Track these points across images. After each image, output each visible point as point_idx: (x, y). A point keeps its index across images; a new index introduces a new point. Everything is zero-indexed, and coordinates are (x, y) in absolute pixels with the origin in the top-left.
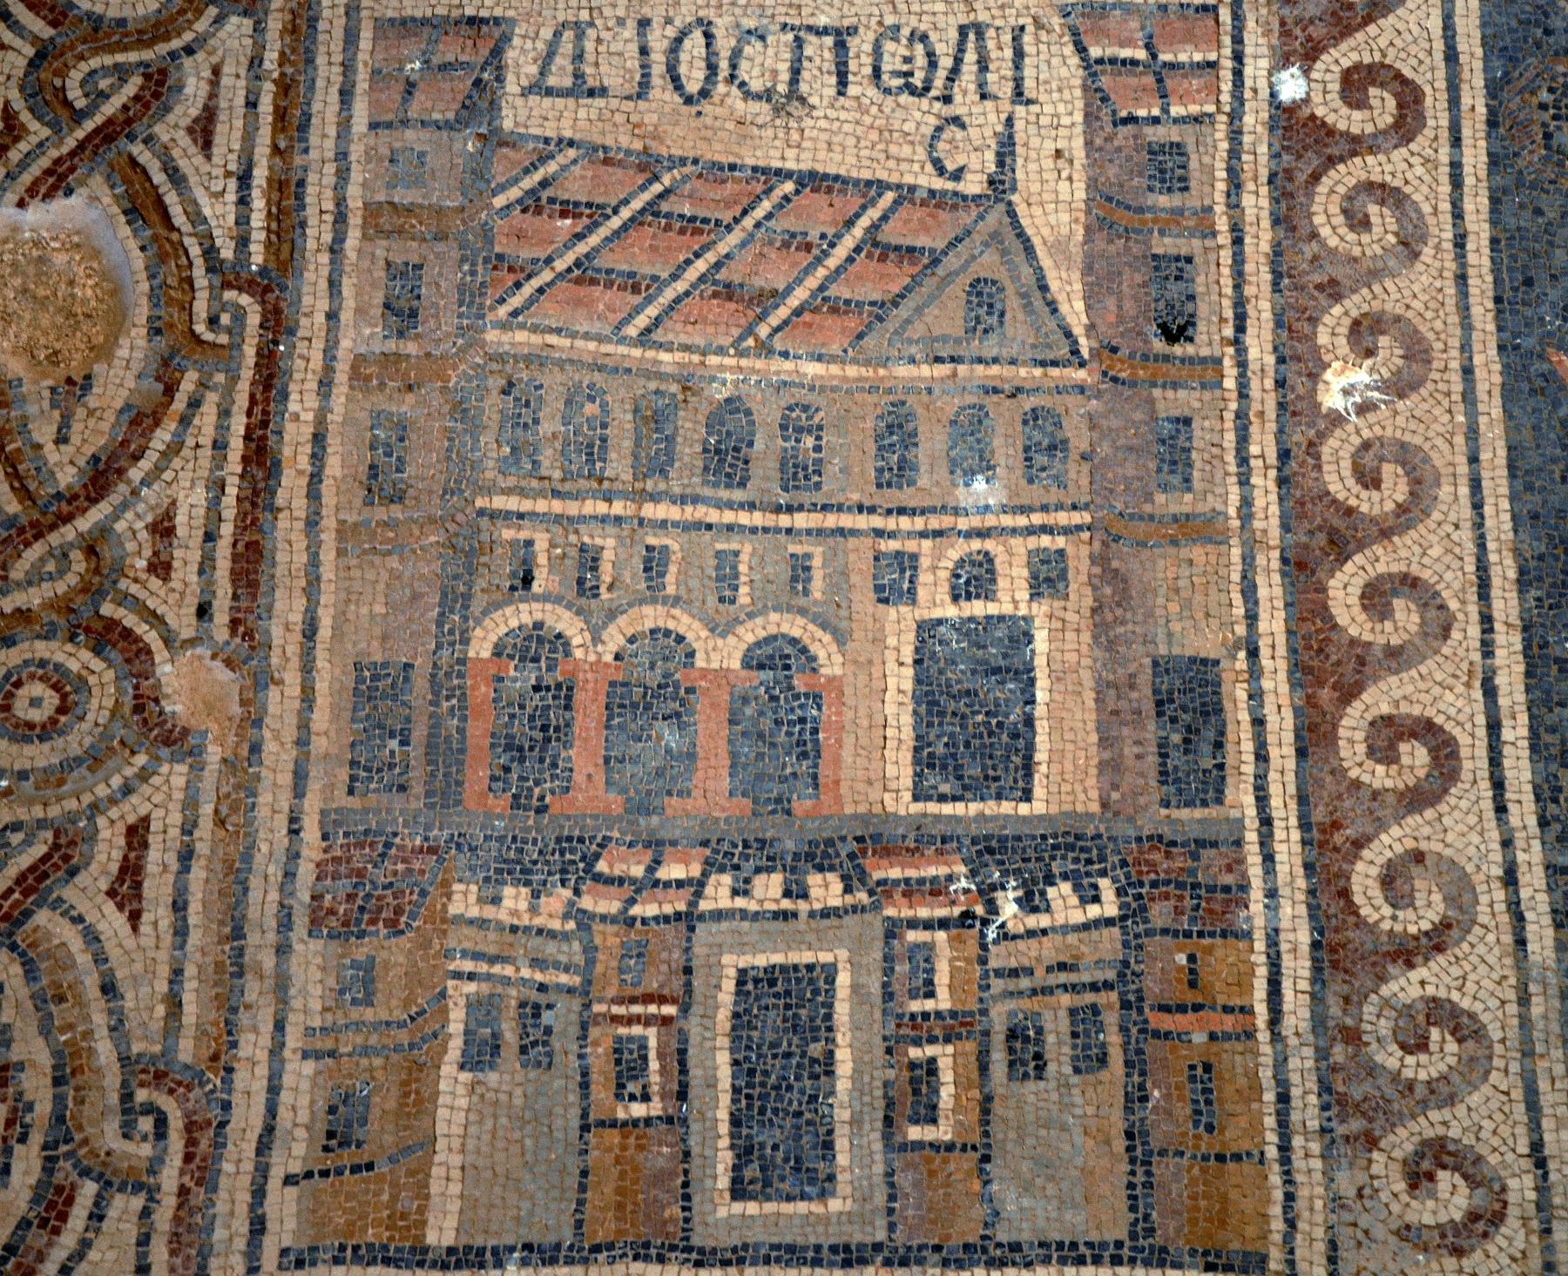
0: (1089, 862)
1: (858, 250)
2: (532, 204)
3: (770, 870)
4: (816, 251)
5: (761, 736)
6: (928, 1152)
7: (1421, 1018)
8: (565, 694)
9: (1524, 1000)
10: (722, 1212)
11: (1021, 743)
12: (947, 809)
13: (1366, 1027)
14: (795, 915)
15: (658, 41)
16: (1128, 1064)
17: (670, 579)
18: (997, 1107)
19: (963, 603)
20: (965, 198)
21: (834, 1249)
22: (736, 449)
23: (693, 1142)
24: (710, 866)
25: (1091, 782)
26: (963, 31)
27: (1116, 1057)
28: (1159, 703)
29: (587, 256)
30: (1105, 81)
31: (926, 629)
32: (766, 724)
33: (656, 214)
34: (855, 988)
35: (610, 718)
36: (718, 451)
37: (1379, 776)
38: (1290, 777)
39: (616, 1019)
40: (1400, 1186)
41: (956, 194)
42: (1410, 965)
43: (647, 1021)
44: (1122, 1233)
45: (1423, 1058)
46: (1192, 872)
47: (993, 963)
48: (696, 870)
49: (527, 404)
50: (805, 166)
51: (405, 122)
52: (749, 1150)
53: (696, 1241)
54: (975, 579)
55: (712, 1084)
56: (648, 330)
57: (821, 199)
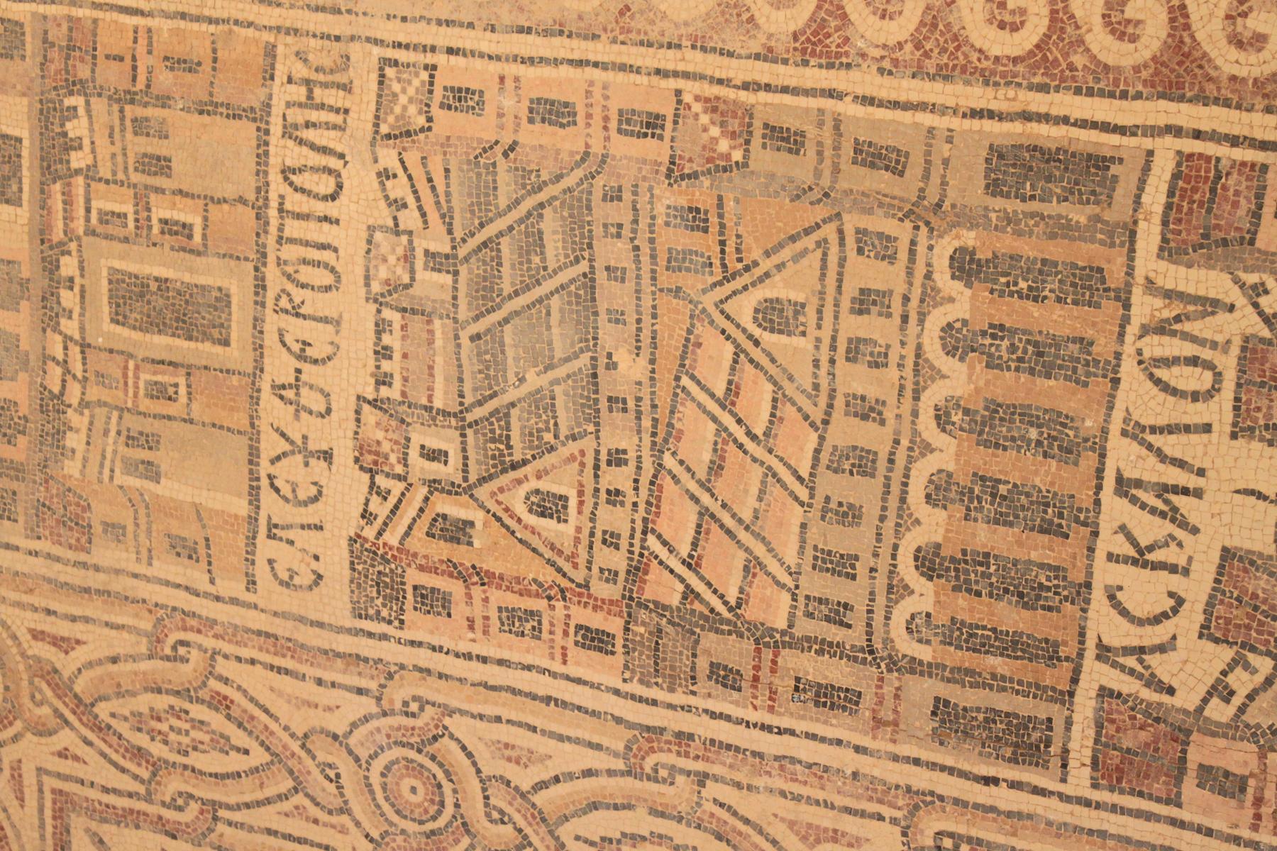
10: (236, 354)
12: (26, 188)
21: (257, 294)
24: (56, 329)
25: (11, 100)
34: (122, 258)
39: (136, 395)
43: (137, 377)
44: (254, 126)
47: (109, 177)
48: (59, 338)
52: (204, 333)
53: (250, 370)
55: (170, 348)
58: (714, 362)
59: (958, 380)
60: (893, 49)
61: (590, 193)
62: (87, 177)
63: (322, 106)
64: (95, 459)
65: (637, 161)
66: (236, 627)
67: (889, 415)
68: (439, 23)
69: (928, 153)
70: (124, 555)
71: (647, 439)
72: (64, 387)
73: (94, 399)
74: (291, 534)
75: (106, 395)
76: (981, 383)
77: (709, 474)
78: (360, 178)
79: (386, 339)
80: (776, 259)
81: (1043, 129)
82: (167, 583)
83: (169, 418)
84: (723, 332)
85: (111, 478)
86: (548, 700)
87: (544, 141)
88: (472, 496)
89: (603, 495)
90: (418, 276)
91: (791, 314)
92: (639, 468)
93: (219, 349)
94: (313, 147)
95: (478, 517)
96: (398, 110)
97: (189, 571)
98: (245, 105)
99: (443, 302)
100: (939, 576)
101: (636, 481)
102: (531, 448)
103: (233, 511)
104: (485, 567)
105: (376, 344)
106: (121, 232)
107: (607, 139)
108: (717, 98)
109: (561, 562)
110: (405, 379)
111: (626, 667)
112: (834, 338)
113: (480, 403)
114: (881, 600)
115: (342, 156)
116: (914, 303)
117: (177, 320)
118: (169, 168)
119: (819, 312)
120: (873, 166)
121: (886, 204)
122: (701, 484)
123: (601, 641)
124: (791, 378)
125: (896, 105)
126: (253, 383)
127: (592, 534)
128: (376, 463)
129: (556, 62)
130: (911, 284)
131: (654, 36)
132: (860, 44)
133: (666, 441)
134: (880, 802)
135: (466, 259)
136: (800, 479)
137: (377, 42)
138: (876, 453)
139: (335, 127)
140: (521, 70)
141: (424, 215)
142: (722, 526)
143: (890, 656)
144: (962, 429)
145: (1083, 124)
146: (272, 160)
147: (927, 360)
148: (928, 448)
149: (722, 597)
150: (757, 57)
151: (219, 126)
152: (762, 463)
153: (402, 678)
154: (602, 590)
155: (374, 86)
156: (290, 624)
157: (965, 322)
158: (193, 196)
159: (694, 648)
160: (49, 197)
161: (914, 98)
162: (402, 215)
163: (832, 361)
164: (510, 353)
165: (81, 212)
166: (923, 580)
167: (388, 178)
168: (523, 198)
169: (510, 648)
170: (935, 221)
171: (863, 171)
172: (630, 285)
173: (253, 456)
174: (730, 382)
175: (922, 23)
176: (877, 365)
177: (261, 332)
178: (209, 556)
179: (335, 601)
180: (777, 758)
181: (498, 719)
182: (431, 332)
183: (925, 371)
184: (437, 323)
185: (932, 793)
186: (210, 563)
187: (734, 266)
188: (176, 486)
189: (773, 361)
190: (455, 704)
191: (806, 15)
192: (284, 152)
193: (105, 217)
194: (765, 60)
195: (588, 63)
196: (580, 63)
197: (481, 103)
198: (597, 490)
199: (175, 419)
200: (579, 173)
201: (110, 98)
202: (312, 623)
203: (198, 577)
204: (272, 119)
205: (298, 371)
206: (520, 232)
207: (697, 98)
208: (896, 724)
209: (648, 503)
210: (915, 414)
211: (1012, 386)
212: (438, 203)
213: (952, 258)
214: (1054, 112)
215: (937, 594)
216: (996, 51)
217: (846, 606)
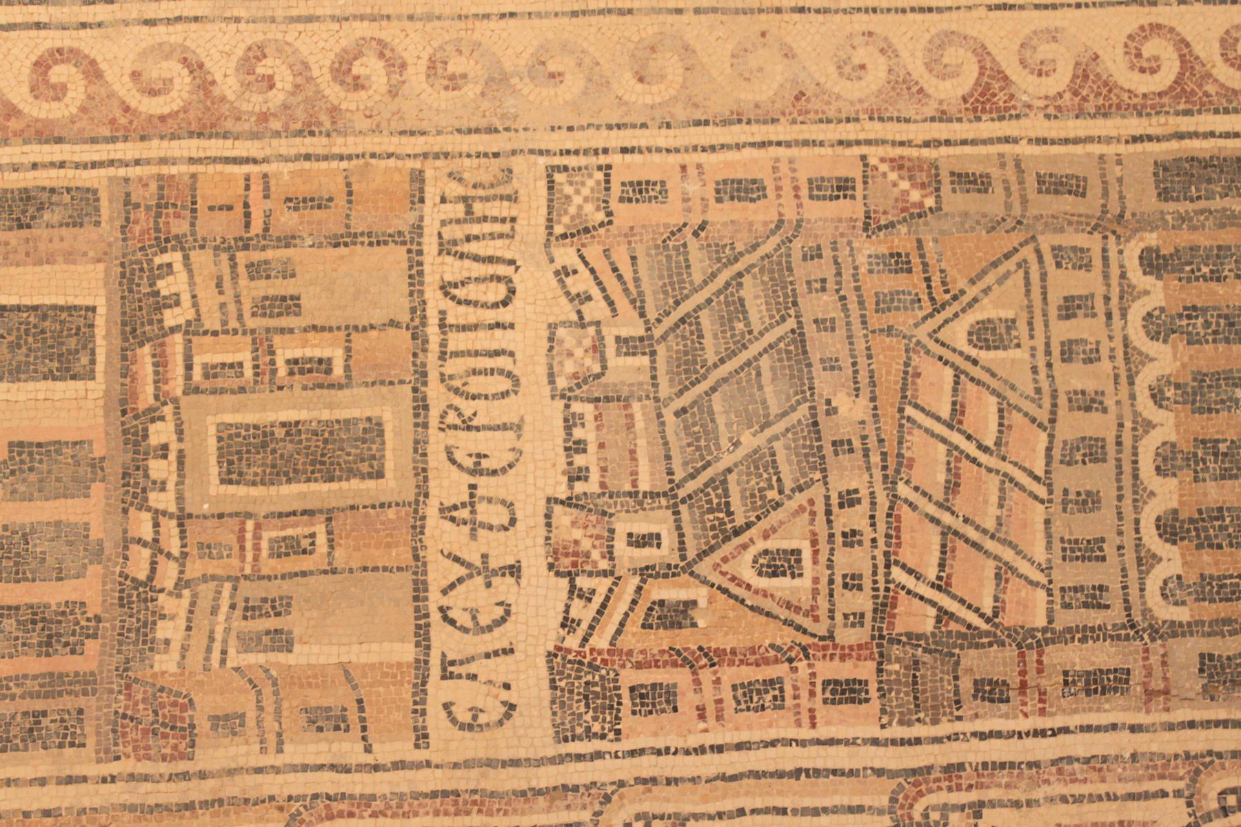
0: (142, 270)
5: (41, 481)
6: (351, 363)
7: (251, 78)
9: (237, 20)
10: (392, 484)
11: (51, 313)
12: (101, 357)
13: (257, 109)
14: (181, 451)
18: (318, 322)
21: (416, 415)
23: (342, 503)
25: (80, 269)
28: (20, 227)
32: (32, 477)
34: (236, 410)
35: (26, 579)
37: (76, 94)
38: (77, 148)
40: (363, 94)
42: (213, 82)
43: (257, 537)
44: (404, 248)
45: (277, 78)
46: (148, 208)
47: (218, 327)
48: (146, 516)
52: (350, 470)
53: (412, 498)
55: (303, 496)
58: (936, 388)
59: (1164, 360)
60: (1054, 98)
61: (789, 255)
62: (187, 333)
63: (485, 219)
64: (198, 641)
65: (832, 220)
66: (401, 796)
67: (1110, 402)
68: (610, 127)
69: (1103, 175)
70: (243, 749)
71: (878, 474)
72: (153, 570)
73: (198, 574)
74: (472, 668)
75: (213, 568)
76: (1186, 359)
77: (946, 493)
78: (535, 282)
79: (578, 433)
80: (981, 285)
81: (1196, 144)
82: (305, 768)
83: (304, 574)
84: (940, 358)
85: (223, 662)
86: (797, 773)
87: (735, 217)
88: (692, 574)
89: (839, 539)
90: (609, 364)
91: (1003, 330)
92: (873, 504)
93: (371, 484)
94: (476, 258)
95: (701, 594)
96: (572, 210)
97: (335, 747)
98: (391, 231)
99: (641, 384)
100: (1182, 539)
101: (872, 517)
102: (754, 509)
103: (394, 659)
104: (713, 645)
105: (566, 441)
106: (235, 383)
107: (800, 206)
108: (902, 158)
109: (799, 619)
110: (604, 469)
111: (883, 711)
112: (1047, 345)
113: (692, 477)
114: (1133, 574)
115: (512, 262)
116: (1115, 301)
117: (313, 463)
118: (298, 306)
119: (1030, 324)
120: (1056, 192)
121: (1075, 222)
122: (940, 505)
123: (853, 691)
124: (1013, 388)
125: (1066, 141)
126: (416, 511)
127: (831, 582)
128: (574, 564)
129: (738, 147)
130: (1108, 285)
131: (831, 114)
132: (1025, 98)
133: (898, 471)
134: (1162, 777)
135: (664, 338)
136: (1037, 479)
137: (541, 152)
138: (1103, 440)
139: (501, 236)
140: (703, 158)
141: (611, 304)
142: (967, 541)
143: (1151, 626)
144: (1176, 402)
145: (1227, 135)
146: (428, 279)
147: (1135, 348)
148: (1149, 425)
149: (977, 610)
150: (933, 119)
151: (361, 255)
152: (998, 472)
153: (621, 797)
154: (848, 636)
155: (543, 192)
156: (474, 773)
157: (1162, 310)
158: (331, 329)
159: (955, 670)
160: (134, 362)
161: (1082, 133)
162: (586, 309)
163: (1049, 365)
164: (721, 420)
165: (180, 370)
166: (1168, 546)
167: (567, 275)
168: (719, 271)
169: (750, 727)
170: (1119, 231)
171: (1048, 197)
172: (841, 332)
173: (420, 590)
174: (954, 403)
175: (1075, 76)
176: (1091, 361)
177: (425, 455)
178: (363, 720)
179: (534, 732)
180: (1054, 762)
181: (741, 812)
182: (630, 417)
183: (1135, 358)
184: (636, 407)
185: (1210, 753)
186: (364, 729)
187: (941, 297)
188: (315, 649)
189: (993, 375)
190: (687, 808)
191: (971, 81)
192: (438, 268)
193: (210, 372)
194: (941, 120)
195: (770, 143)
196: (763, 145)
197: (664, 192)
198: (831, 536)
199: (312, 573)
200: (775, 240)
201: (216, 248)
202: (504, 764)
203: (349, 749)
204: (425, 240)
205: (473, 487)
206: (719, 303)
207: (882, 160)
208: (1166, 692)
209: (888, 536)
210: (1133, 397)
211: (1212, 356)
212: (626, 290)
213: (1141, 258)
214: (1201, 129)
215: (1183, 555)
216: (1142, 89)
217: (1101, 588)
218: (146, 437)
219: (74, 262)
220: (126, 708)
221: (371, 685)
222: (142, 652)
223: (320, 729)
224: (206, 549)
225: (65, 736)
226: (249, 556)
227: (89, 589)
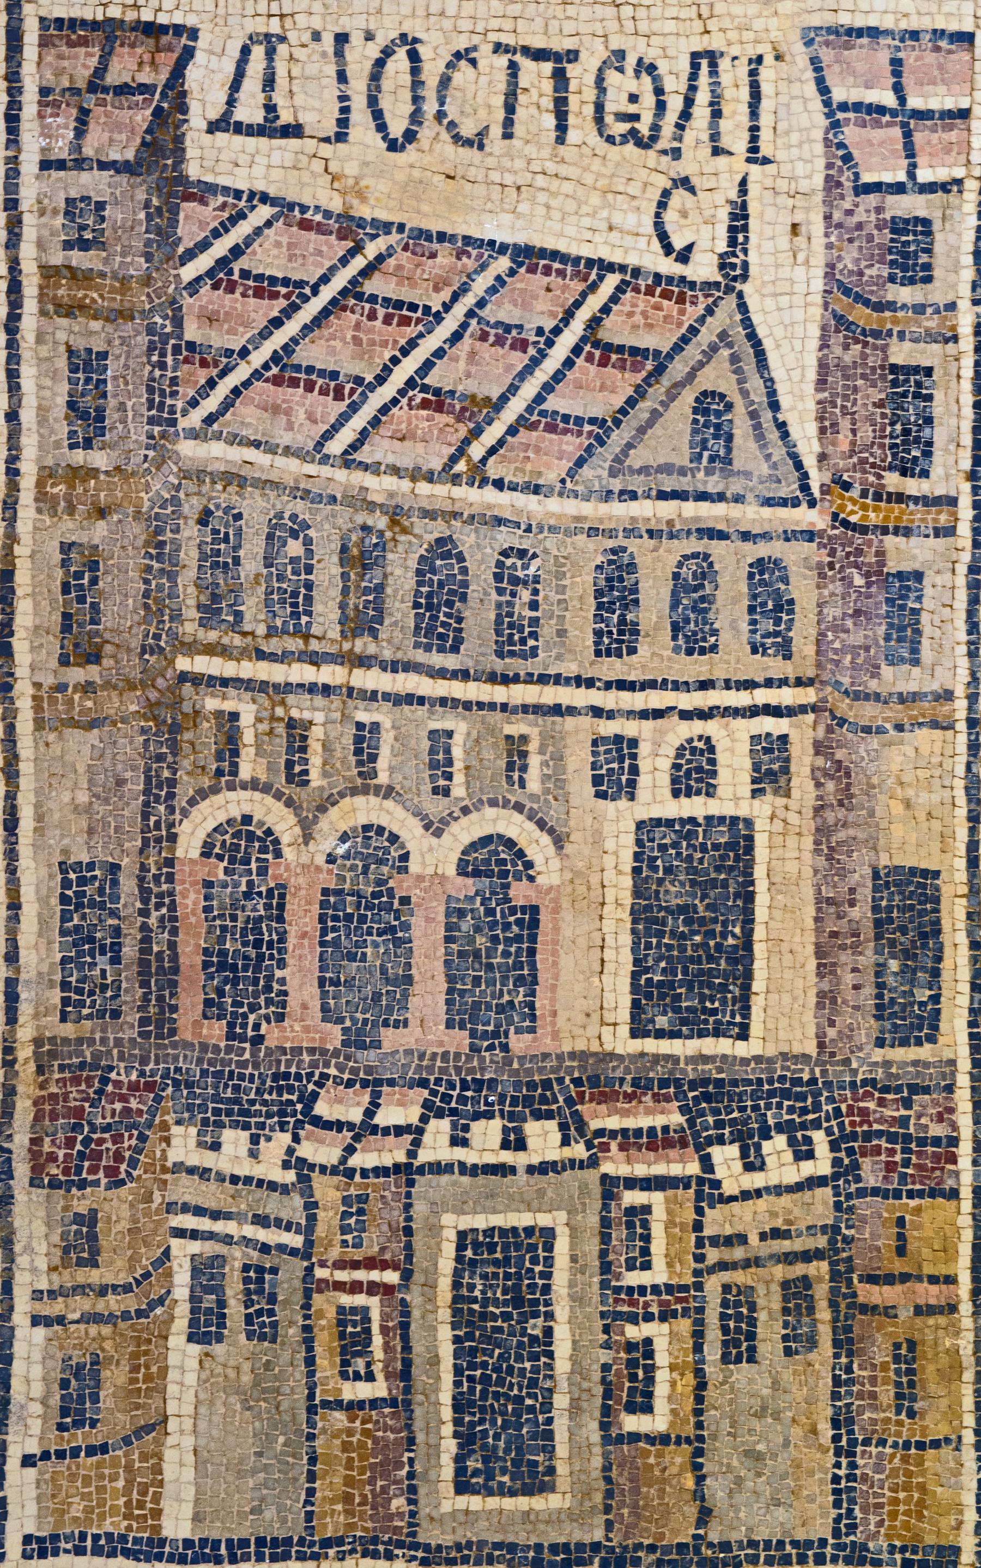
0: (804, 1111)
1: (577, 350)
2: (221, 275)
3: (489, 1115)
4: (532, 351)
5: (477, 954)
8: (277, 901)
10: (446, 1507)
14: (513, 1170)
15: (360, 57)
16: (836, 1343)
17: (382, 764)
18: (711, 1393)
19: (683, 799)
20: (692, 285)
22: (450, 604)
26: (695, 57)
27: (825, 1333)
28: (878, 923)
29: (285, 347)
30: (850, 134)
31: (646, 828)
32: (481, 941)
33: (359, 296)
35: (324, 932)
36: (429, 607)
39: (339, 1286)
41: (683, 279)
43: (372, 1288)
47: (707, 1232)
48: (412, 1115)
49: (226, 539)
50: (521, 238)
51: (80, 164)
53: (421, 1538)
54: (695, 771)
55: (435, 1361)
56: (355, 446)
57: (539, 280)
62: (701, 1181)
64: (211, 1195)
70: (42, 1264)
72: (328, 1125)
73: (318, 1196)
75: (327, 1220)
85: (180, 1233)
93: (448, 1471)
97: (36, 1408)
98: (857, 1512)
117: (485, 1379)
118: (738, 1360)
126: (400, 1544)
158: (698, 1412)
165: (641, 1170)
178: (75, 1452)
186: (61, 1455)
188: (191, 1379)
199: (311, 1374)
201: (836, 1229)
218: (539, 1116)
219: (820, 1005)
220: (118, 1084)
221: (129, 1468)
222: (203, 1108)
223: (64, 1384)
224: (356, 1207)
225: (79, 991)
226: (342, 1276)
227: (303, 1022)
